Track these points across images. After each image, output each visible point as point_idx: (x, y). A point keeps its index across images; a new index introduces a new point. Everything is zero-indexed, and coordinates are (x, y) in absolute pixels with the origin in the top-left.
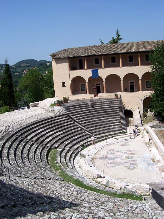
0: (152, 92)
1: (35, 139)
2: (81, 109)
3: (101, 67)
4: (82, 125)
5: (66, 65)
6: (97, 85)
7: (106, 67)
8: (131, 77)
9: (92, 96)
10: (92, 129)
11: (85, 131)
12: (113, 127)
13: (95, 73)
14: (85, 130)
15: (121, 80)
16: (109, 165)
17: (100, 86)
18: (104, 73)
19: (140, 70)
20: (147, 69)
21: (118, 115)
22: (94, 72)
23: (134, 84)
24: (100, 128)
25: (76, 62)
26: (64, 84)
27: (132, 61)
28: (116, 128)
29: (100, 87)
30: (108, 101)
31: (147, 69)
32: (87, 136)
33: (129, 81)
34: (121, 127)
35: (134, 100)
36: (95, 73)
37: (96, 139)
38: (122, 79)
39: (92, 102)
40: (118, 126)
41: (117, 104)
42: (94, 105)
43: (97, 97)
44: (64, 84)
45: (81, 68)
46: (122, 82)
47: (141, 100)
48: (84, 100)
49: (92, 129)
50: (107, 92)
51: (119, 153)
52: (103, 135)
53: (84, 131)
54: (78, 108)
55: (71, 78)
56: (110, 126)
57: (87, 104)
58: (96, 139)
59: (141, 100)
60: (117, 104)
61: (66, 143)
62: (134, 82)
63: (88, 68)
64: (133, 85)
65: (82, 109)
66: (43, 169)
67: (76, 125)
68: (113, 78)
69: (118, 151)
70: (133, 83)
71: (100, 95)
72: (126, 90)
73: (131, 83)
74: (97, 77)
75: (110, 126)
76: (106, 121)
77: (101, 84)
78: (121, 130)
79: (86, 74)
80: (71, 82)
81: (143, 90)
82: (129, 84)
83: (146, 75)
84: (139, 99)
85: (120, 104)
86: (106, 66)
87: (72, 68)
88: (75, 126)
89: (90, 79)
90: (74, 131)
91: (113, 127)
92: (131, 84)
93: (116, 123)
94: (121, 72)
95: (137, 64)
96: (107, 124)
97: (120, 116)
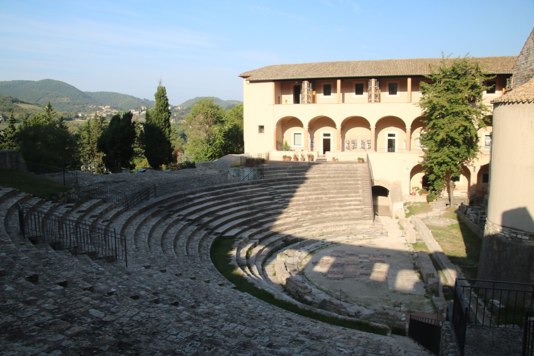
1: (193, 217)
23: (396, 138)
26: (261, 128)
29: (329, 140)
44: (261, 128)
47: (407, 169)
59: (407, 169)
66: (199, 265)
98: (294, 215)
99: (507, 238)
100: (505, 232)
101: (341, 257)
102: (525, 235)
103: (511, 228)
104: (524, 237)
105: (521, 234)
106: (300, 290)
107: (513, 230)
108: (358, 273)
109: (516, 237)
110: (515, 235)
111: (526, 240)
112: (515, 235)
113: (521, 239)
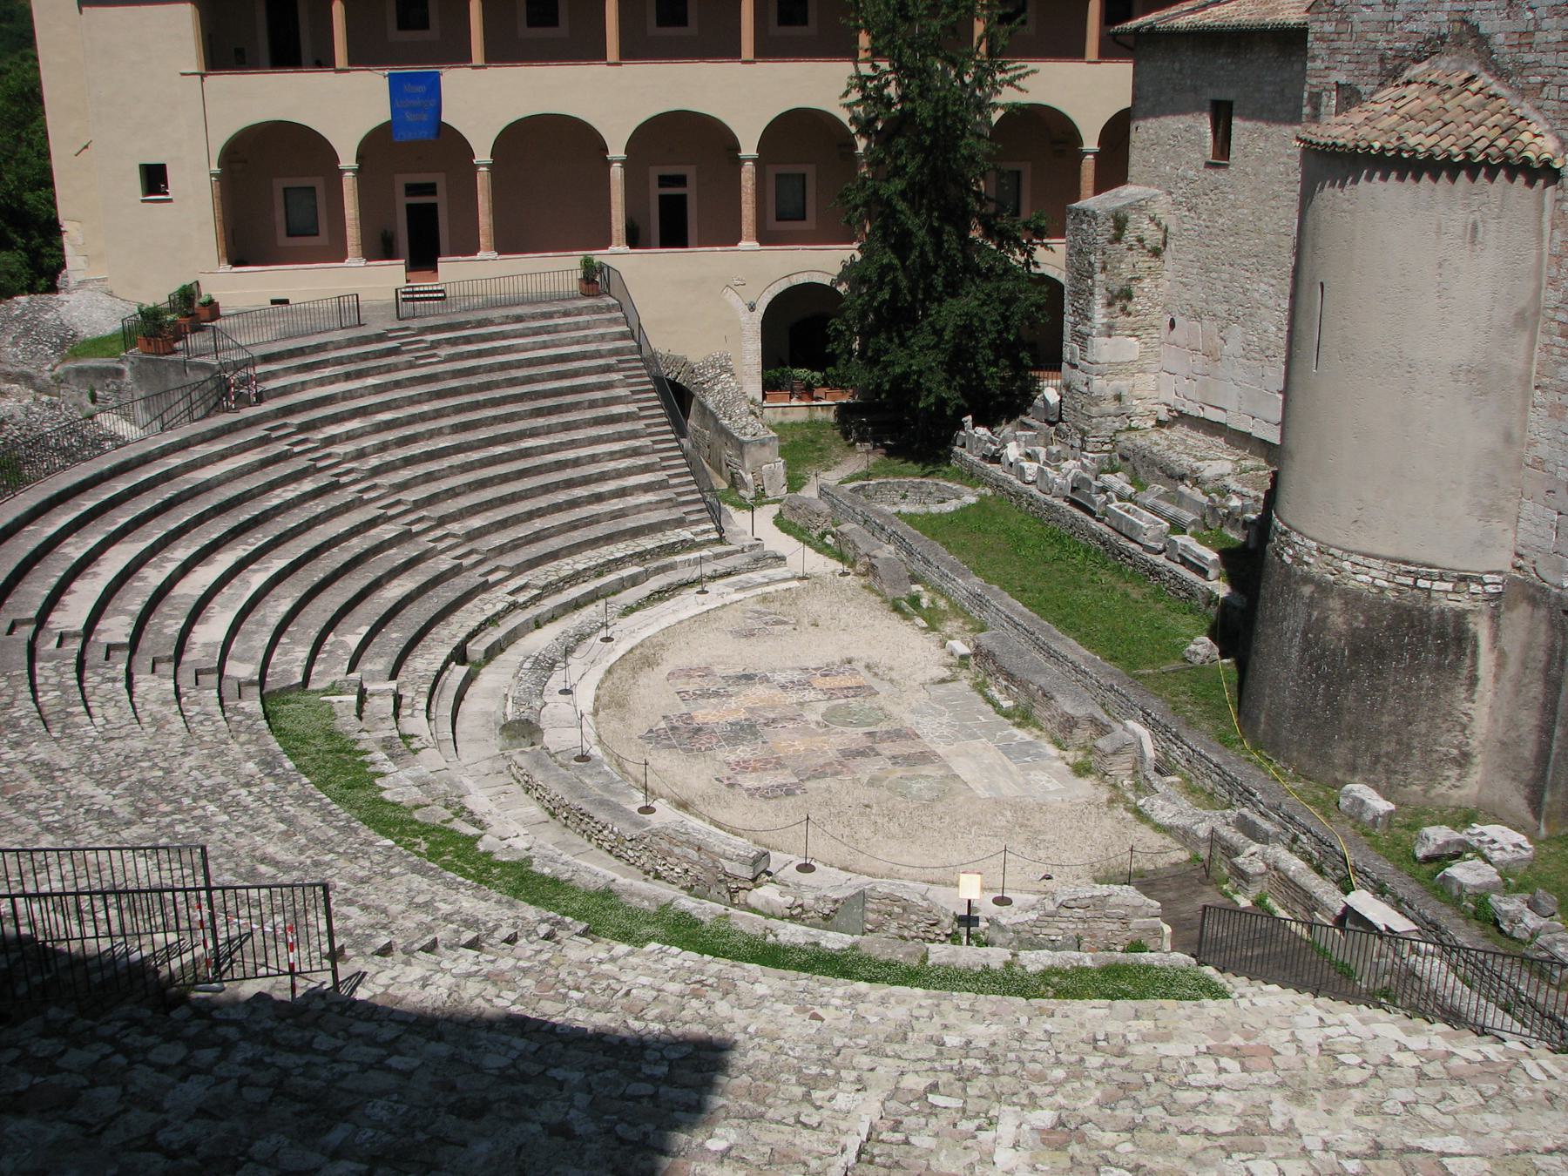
0: (849, 252)
2: (348, 376)
3: (461, 56)
4: (398, 502)
6: (412, 189)
8: (682, 140)
9: (391, 275)
10: (476, 522)
11: (441, 546)
12: (615, 504)
13: (414, 98)
14: (432, 535)
15: (608, 164)
16: (785, 777)
17: (441, 200)
21: (628, 417)
22: (408, 88)
23: (691, 191)
24: (531, 515)
26: (154, 179)
27: (682, 21)
28: (638, 509)
30: (534, 312)
32: (461, 584)
33: (654, 173)
34: (672, 503)
36: (414, 98)
37: (535, 599)
38: (617, 151)
39: (416, 324)
40: (651, 497)
41: (602, 338)
42: (435, 345)
43: (423, 283)
46: (617, 172)
47: (752, 308)
48: (351, 311)
49: (476, 522)
50: (507, 244)
51: (758, 694)
52: (567, 566)
53: (424, 543)
54: (327, 372)
56: (599, 498)
57: (380, 338)
58: (535, 599)
59: (752, 308)
60: (602, 338)
61: (343, 645)
62: (690, 172)
63: (361, 58)
64: (683, 198)
65: (360, 374)
67: (358, 503)
68: (548, 144)
69: (749, 678)
70: (680, 181)
71: (452, 272)
72: (635, 239)
75: (599, 498)
76: (561, 465)
78: (680, 523)
80: (215, 168)
81: (766, 237)
82: (655, 192)
83: (796, 131)
85: (630, 336)
86: (502, 52)
87: (224, 52)
88: (347, 507)
89: (374, 146)
90: (357, 545)
91: (615, 504)
92: (681, 190)
93: (629, 472)
95: (592, 51)
96: (569, 484)
97: (640, 425)
98: (441, 546)
99: (1382, 590)
100: (1374, 573)
101: (716, 694)
102: (1441, 579)
103: (1393, 560)
104: (1437, 585)
105: (1428, 576)
106: (729, 866)
107: (1403, 567)
108: (832, 754)
109: (1415, 586)
110: (1410, 581)
111: (1446, 592)
112: (1410, 581)
113: (1429, 590)
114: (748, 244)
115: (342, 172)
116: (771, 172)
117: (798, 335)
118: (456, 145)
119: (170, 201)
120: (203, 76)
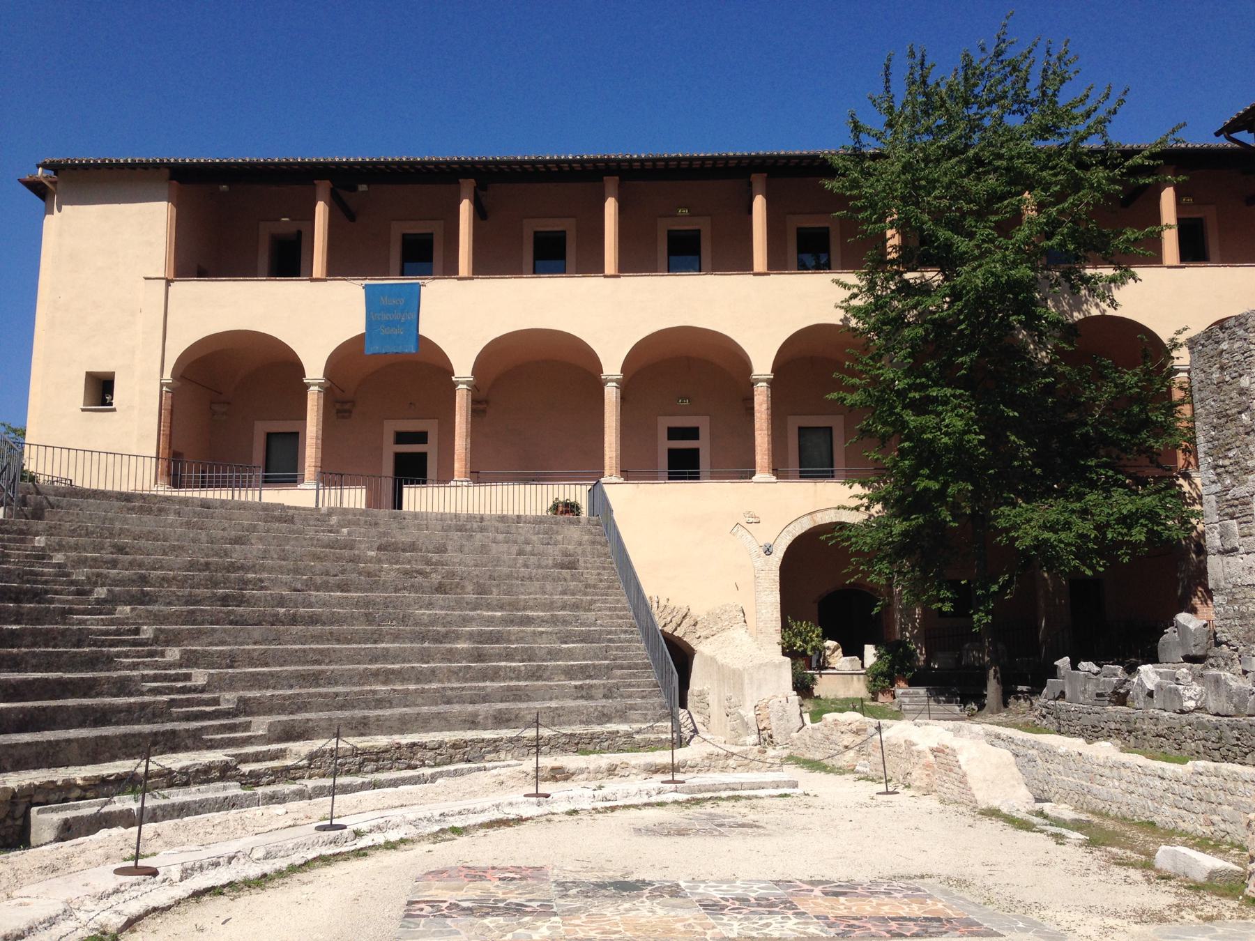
5: (148, 225)
7: (486, 265)
13: (396, 314)
17: (430, 449)
18: (466, 314)
19: (763, 309)
20: (821, 298)
23: (703, 445)
25: (233, 220)
26: (101, 389)
31: (821, 298)
33: (665, 423)
35: (712, 546)
44: (101, 389)
45: (288, 262)
47: (768, 551)
55: (178, 345)
59: (768, 551)
63: (338, 268)
70: (693, 433)
71: (416, 498)
73: (674, 433)
74: (411, 348)
77: (433, 438)
79: (315, 316)
80: (168, 377)
81: (780, 471)
84: (751, 542)
89: (344, 359)
92: (688, 410)
94: (611, 312)
114: (762, 475)
115: (307, 386)
116: (794, 423)
117: (824, 596)
118: (434, 365)
119: (114, 410)
120: (168, 282)
